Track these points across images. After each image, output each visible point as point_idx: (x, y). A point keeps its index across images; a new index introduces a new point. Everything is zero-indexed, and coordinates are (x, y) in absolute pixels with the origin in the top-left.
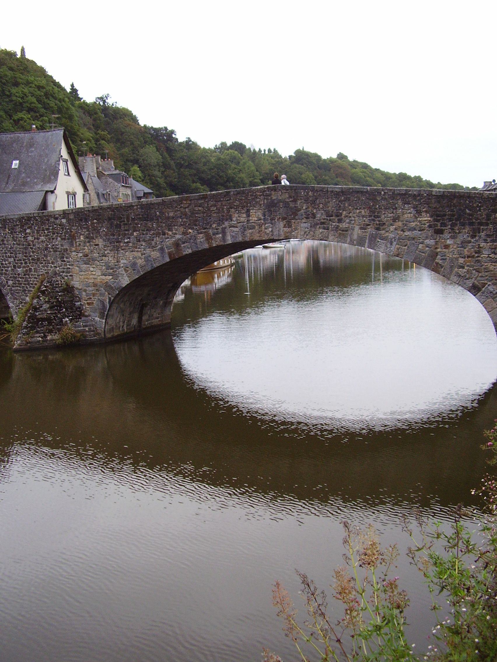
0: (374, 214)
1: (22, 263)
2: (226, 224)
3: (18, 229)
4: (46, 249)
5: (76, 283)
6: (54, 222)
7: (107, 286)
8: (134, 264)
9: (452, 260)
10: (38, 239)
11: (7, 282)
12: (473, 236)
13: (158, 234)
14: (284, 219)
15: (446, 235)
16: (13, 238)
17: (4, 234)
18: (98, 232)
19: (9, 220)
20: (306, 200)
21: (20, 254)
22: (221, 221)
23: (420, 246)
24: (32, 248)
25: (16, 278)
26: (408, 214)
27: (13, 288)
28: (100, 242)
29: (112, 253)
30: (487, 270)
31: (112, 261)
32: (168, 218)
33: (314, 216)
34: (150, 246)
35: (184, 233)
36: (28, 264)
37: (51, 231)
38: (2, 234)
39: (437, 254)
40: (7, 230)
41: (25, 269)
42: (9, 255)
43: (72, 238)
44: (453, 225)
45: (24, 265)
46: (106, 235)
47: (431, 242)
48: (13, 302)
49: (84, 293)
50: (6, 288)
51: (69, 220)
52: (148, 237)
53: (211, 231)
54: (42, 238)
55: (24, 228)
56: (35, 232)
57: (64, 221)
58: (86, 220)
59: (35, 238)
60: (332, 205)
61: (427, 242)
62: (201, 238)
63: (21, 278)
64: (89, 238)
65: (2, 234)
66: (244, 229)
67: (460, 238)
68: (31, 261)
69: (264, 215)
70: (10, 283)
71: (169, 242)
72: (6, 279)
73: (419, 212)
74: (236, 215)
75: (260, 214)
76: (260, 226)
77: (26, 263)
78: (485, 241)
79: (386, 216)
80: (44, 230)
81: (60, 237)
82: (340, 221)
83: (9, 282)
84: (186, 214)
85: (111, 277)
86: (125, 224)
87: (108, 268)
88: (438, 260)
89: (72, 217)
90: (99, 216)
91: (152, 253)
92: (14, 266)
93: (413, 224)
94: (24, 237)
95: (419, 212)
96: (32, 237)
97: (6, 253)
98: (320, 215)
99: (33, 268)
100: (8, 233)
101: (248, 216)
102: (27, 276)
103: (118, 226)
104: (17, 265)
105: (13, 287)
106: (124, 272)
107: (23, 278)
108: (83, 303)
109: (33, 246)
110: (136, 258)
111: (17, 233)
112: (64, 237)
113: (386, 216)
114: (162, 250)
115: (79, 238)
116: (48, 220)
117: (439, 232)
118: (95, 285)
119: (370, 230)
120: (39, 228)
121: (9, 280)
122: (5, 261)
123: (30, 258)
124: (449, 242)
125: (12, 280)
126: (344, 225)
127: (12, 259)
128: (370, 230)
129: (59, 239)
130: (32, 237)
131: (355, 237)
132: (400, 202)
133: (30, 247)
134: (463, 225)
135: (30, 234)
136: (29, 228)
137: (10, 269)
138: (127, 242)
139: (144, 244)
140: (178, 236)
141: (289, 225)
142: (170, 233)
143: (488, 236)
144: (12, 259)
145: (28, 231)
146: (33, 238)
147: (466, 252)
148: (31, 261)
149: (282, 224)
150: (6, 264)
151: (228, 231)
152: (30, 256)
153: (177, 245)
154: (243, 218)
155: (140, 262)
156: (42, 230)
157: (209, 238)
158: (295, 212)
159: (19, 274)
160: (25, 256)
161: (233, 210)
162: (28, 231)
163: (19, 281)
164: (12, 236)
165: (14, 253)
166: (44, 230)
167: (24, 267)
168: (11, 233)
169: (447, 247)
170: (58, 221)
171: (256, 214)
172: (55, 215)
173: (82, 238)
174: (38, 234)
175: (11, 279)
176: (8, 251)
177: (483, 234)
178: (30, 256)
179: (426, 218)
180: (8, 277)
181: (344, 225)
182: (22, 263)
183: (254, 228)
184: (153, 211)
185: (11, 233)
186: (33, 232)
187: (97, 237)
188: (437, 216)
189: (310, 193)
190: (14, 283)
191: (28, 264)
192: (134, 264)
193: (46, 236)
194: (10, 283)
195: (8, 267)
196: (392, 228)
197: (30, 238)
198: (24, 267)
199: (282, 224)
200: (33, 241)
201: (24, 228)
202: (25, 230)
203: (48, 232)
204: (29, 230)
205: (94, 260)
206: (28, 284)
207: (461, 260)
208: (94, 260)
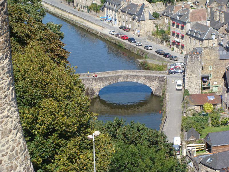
0: (138, 78)
7: (99, 88)
8: (104, 85)
22: (117, 79)
26: (142, 78)
43: (93, 82)
58: (96, 79)
62: (114, 81)
66: (120, 80)
79: (139, 78)
108: (95, 91)
114: (108, 83)
119: (137, 80)
128: (137, 80)
153: (111, 82)
155: (105, 85)
157: (115, 81)
158: (128, 78)
171: (122, 78)
179: (144, 78)
192: (104, 85)
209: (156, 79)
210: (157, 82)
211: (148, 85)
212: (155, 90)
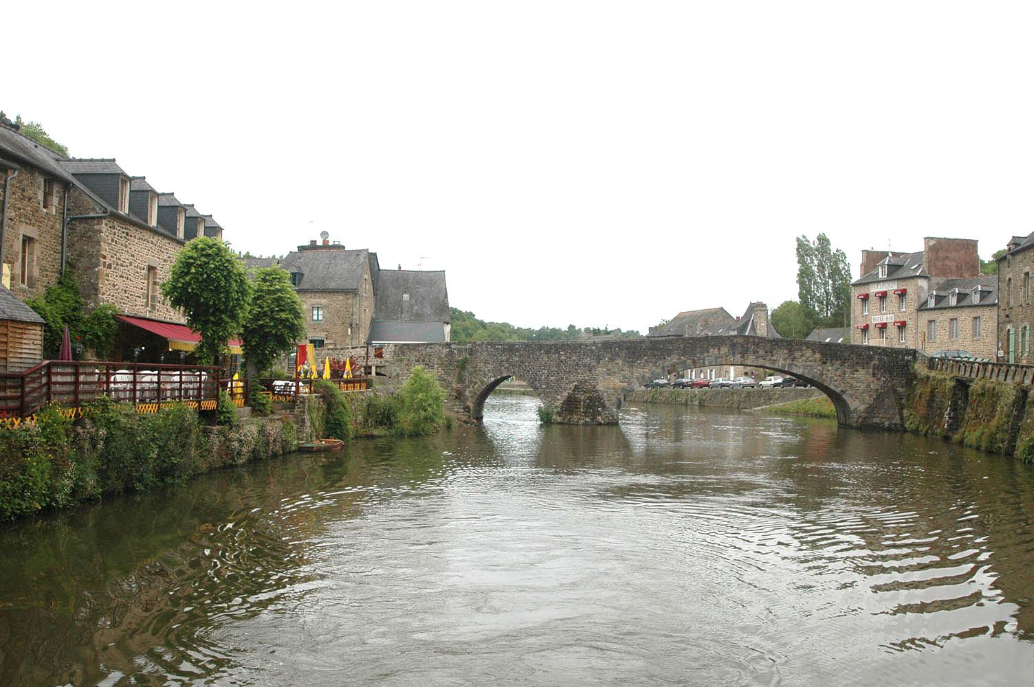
0: (791, 352)
2: (706, 354)
3: (553, 351)
4: (577, 364)
5: (600, 387)
8: (643, 377)
9: (831, 378)
12: (841, 366)
13: (661, 359)
14: (740, 353)
15: (828, 364)
18: (619, 356)
20: (754, 343)
22: (702, 353)
23: (815, 370)
26: (809, 353)
28: (620, 362)
29: (628, 369)
30: (848, 383)
31: (627, 373)
33: (758, 352)
34: (655, 365)
39: (823, 375)
44: (832, 360)
47: (821, 368)
49: (606, 394)
52: (654, 360)
53: (696, 359)
54: (574, 358)
57: (594, 348)
60: (768, 348)
61: (818, 368)
64: (612, 360)
67: (835, 367)
69: (729, 350)
70: (544, 386)
73: (814, 353)
74: (711, 350)
75: (726, 350)
76: (727, 356)
78: (848, 368)
82: (772, 356)
84: (680, 348)
85: (626, 384)
87: (624, 378)
88: (824, 377)
89: (600, 345)
92: (548, 376)
93: (812, 359)
95: (814, 353)
98: (761, 352)
106: (636, 381)
110: (645, 372)
113: (797, 354)
114: (663, 368)
117: (825, 363)
118: (614, 388)
124: (830, 368)
126: (774, 358)
127: (546, 371)
129: (589, 359)
131: (780, 364)
132: (804, 347)
134: (837, 360)
138: (640, 363)
140: (674, 361)
141: (743, 357)
142: (669, 358)
143: (848, 366)
144: (546, 371)
145: (562, 353)
147: (838, 373)
149: (739, 356)
151: (706, 359)
154: (716, 351)
162: (561, 353)
169: (828, 371)
170: (588, 348)
173: (607, 359)
177: (846, 365)
179: (818, 355)
181: (774, 358)
183: (722, 357)
188: (823, 355)
189: (756, 340)
196: (800, 360)
199: (739, 356)
205: (614, 373)
206: (560, 388)
207: (836, 378)
208: (614, 373)
209: (871, 358)
210: (874, 375)
211: (832, 387)
212: (862, 408)
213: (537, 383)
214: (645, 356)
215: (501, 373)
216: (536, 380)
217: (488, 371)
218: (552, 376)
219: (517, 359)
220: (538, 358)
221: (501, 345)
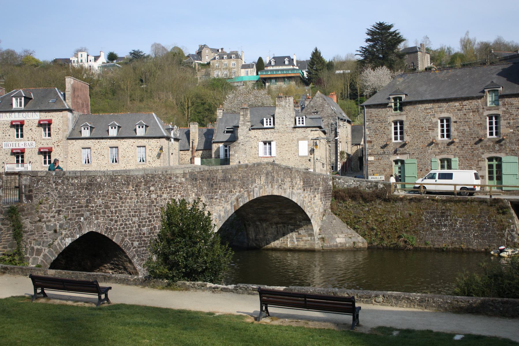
1: (146, 222)
3: (143, 187)
6: (175, 181)
10: (161, 196)
11: (132, 244)
15: (306, 192)
16: (137, 195)
17: (127, 191)
19: (132, 176)
21: (144, 212)
24: (155, 206)
25: (142, 237)
27: (139, 249)
32: (234, 180)
35: (240, 192)
36: (152, 222)
37: (172, 188)
38: (125, 192)
40: (131, 187)
41: (149, 228)
42: (134, 213)
45: (148, 223)
46: (206, 193)
48: (140, 265)
50: (132, 250)
51: (186, 179)
54: (165, 196)
55: (148, 186)
56: (158, 189)
57: (183, 180)
59: (157, 195)
63: (146, 237)
65: (125, 192)
68: (155, 219)
71: (234, 198)
72: (131, 241)
77: (150, 221)
80: (166, 188)
81: (180, 194)
83: (134, 243)
86: (215, 184)
89: (188, 177)
90: (202, 176)
91: (227, 206)
92: (139, 226)
94: (148, 194)
96: (155, 194)
97: (130, 212)
98: (280, 181)
99: (157, 226)
100: (132, 190)
101: (261, 180)
102: (151, 234)
103: (212, 185)
104: (141, 224)
105: (139, 247)
107: (148, 237)
109: (157, 203)
111: (141, 190)
112: (183, 194)
115: (192, 196)
116: (170, 178)
120: (162, 185)
121: (134, 241)
122: (128, 221)
123: (154, 216)
125: (138, 241)
127: (137, 219)
130: (155, 194)
133: (153, 204)
135: (153, 191)
136: (153, 185)
137: (134, 229)
138: (217, 198)
139: (224, 200)
140: (237, 194)
144: (137, 219)
145: (152, 188)
146: (156, 195)
148: (155, 219)
150: (130, 224)
152: (154, 214)
156: (164, 188)
159: (144, 234)
160: (150, 214)
161: (256, 176)
162: (152, 188)
163: (145, 241)
164: (136, 194)
165: (138, 211)
166: (166, 188)
167: (149, 226)
168: (135, 190)
172: (176, 174)
174: (161, 192)
175: (136, 240)
176: (132, 209)
178: (154, 214)
179: (302, 183)
180: (133, 238)
182: (146, 222)
184: (227, 175)
185: (135, 190)
186: (156, 190)
187: (202, 194)
190: (139, 244)
191: (152, 222)
192: (220, 216)
193: (168, 193)
194: (136, 244)
195: (132, 227)
197: (153, 196)
198: (149, 226)
200: (156, 199)
201: (148, 186)
202: (149, 187)
203: (170, 190)
204: (153, 187)
213: (127, 239)
214: (220, 189)
215: (80, 228)
216: (126, 235)
217: (61, 226)
218: (144, 226)
219: (99, 201)
220: (126, 199)
221: (76, 178)
